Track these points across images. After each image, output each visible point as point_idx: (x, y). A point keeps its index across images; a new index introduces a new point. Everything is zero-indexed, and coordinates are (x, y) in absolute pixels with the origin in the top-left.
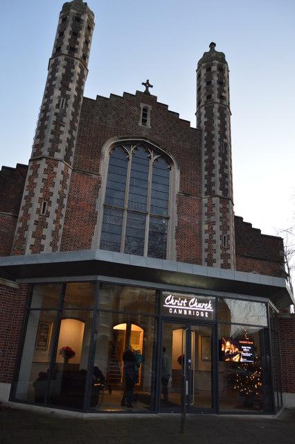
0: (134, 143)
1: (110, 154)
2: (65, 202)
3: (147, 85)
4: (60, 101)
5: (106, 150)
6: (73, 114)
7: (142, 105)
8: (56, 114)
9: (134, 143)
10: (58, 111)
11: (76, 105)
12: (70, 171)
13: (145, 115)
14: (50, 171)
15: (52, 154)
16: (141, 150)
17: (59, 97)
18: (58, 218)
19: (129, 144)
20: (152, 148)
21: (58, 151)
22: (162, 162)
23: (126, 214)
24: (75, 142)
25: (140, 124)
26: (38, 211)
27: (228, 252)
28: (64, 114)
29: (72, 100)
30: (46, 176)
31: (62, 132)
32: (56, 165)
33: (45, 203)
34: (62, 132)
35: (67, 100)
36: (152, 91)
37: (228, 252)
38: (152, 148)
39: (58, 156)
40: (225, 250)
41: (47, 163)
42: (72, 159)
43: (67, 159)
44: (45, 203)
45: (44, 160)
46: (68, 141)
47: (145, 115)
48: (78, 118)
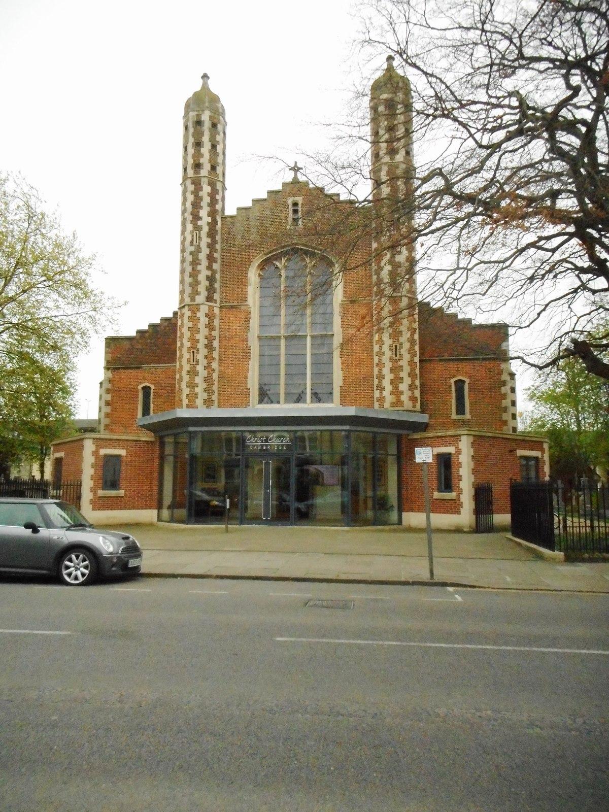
1: (260, 275)
2: (216, 344)
4: (193, 236)
6: (209, 246)
11: (212, 234)
12: (217, 311)
14: (194, 318)
15: (193, 299)
17: (192, 232)
18: (209, 363)
21: (198, 294)
24: (218, 276)
26: (189, 360)
27: (401, 363)
28: (199, 249)
29: (206, 229)
30: (190, 324)
31: (199, 272)
32: (198, 310)
33: (193, 352)
34: (199, 272)
35: (200, 233)
37: (401, 363)
40: (396, 361)
41: (190, 310)
42: (217, 296)
43: (209, 298)
44: (193, 352)
45: (187, 307)
46: (208, 278)
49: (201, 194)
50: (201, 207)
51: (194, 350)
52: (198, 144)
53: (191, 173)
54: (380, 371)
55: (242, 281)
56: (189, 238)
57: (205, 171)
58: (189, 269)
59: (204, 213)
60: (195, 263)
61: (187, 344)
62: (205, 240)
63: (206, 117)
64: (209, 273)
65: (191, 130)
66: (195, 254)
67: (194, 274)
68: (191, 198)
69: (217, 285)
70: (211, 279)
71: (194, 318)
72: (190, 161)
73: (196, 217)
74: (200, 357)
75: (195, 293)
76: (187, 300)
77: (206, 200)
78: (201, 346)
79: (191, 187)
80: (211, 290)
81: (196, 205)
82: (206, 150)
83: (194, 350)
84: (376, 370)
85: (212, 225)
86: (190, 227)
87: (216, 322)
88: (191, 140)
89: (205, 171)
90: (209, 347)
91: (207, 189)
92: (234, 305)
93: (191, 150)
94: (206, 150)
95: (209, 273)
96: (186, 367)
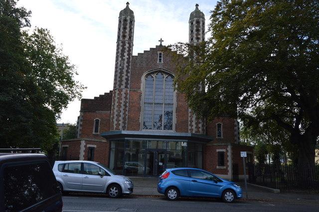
0: (156, 72)
2: (128, 104)
3: (161, 41)
5: (143, 78)
7: (159, 52)
8: (120, 69)
9: (156, 72)
10: (121, 67)
11: (128, 62)
12: (128, 92)
13: (160, 57)
14: (120, 94)
15: (120, 87)
16: (160, 74)
18: (125, 112)
19: (153, 73)
20: (164, 72)
22: (170, 77)
23: (153, 104)
24: (129, 78)
25: (158, 62)
28: (123, 68)
29: (126, 60)
32: (122, 91)
36: (163, 44)
38: (164, 72)
39: (123, 87)
42: (129, 86)
43: (126, 87)
47: (160, 57)
48: (130, 67)
49: (125, 47)
50: (125, 52)
51: (119, 106)
52: (125, 28)
53: (121, 39)
54: (191, 119)
55: (139, 81)
56: (119, 63)
57: (127, 39)
58: (119, 75)
59: (126, 54)
60: (121, 73)
61: (117, 104)
62: (126, 64)
63: (128, 18)
64: (126, 77)
65: (122, 23)
66: (122, 69)
67: (121, 77)
68: (121, 48)
69: (129, 82)
70: (127, 79)
71: (120, 94)
72: (121, 34)
73: (123, 55)
74: (122, 109)
75: (120, 85)
76: (118, 87)
77: (127, 49)
78: (122, 105)
79: (121, 44)
80: (127, 83)
81: (123, 51)
82: (127, 31)
83: (119, 106)
84: (189, 119)
85: (128, 59)
86: (120, 59)
87: (128, 96)
88: (122, 26)
89: (127, 39)
90: (125, 105)
91: (127, 45)
92: (136, 88)
93: (122, 30)
94: (127, 31)
95: (126, 77)
96: (116, 113)
